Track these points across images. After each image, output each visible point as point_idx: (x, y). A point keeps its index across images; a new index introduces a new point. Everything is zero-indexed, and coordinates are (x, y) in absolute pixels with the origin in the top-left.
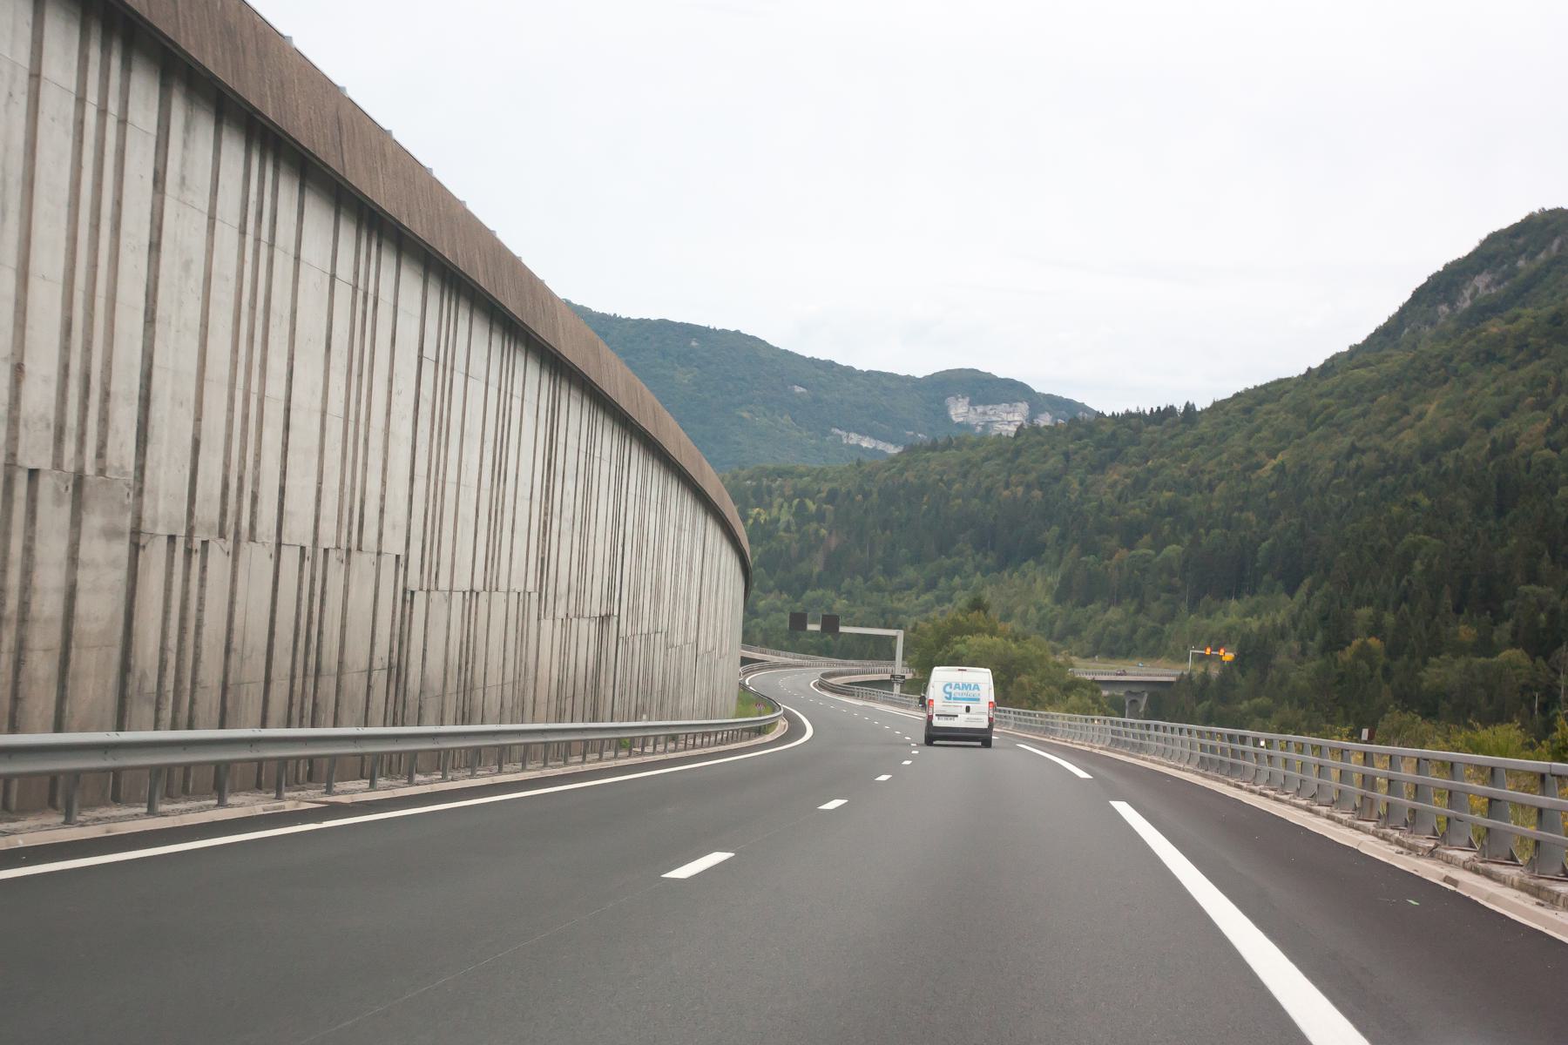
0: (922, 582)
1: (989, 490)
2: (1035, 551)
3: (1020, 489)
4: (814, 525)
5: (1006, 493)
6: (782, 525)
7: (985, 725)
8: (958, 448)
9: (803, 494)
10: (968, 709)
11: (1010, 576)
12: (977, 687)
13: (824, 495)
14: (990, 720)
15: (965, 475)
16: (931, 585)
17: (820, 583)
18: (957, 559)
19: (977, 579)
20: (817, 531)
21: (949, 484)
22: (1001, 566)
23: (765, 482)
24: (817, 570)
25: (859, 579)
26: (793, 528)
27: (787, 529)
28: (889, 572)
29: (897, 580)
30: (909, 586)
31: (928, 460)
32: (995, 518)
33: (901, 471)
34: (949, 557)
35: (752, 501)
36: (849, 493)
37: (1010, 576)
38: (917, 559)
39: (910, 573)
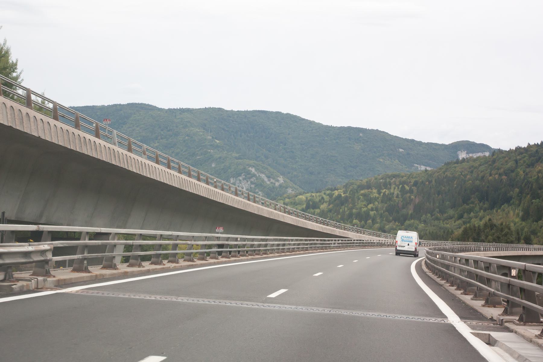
0: (456, 216)
1: (483, 177)
2: (508, 200)
3: (497, 176)
4: (409, 195)
5: (490, 178)
6: (395, 195)
7: (414, 250)
8: (468, 162)
10: (408, 245)
11: (497, 211)
12: (412, 238)
13: (412, 183)
14: (416, 248)
15: (472, 172)
16: (461, 217)
17: (412, 217)
18: (471, 205)
19: (481, 213)
20: (410, 197)
21: (465, 176)
22: (492, 207)
23: (388, 180)
24: (410, 212)
25: (429, 215)
26: (400, 196)
27: (397, 197)
28: (442, 212)
29: (446, 215)
31: (455, 167)
32: (488, 187)
33: (444, 173)
34: (468, 204)
36: (422, 182)
37: (497, 211)
38: (453, 206)
39: (451, 212)
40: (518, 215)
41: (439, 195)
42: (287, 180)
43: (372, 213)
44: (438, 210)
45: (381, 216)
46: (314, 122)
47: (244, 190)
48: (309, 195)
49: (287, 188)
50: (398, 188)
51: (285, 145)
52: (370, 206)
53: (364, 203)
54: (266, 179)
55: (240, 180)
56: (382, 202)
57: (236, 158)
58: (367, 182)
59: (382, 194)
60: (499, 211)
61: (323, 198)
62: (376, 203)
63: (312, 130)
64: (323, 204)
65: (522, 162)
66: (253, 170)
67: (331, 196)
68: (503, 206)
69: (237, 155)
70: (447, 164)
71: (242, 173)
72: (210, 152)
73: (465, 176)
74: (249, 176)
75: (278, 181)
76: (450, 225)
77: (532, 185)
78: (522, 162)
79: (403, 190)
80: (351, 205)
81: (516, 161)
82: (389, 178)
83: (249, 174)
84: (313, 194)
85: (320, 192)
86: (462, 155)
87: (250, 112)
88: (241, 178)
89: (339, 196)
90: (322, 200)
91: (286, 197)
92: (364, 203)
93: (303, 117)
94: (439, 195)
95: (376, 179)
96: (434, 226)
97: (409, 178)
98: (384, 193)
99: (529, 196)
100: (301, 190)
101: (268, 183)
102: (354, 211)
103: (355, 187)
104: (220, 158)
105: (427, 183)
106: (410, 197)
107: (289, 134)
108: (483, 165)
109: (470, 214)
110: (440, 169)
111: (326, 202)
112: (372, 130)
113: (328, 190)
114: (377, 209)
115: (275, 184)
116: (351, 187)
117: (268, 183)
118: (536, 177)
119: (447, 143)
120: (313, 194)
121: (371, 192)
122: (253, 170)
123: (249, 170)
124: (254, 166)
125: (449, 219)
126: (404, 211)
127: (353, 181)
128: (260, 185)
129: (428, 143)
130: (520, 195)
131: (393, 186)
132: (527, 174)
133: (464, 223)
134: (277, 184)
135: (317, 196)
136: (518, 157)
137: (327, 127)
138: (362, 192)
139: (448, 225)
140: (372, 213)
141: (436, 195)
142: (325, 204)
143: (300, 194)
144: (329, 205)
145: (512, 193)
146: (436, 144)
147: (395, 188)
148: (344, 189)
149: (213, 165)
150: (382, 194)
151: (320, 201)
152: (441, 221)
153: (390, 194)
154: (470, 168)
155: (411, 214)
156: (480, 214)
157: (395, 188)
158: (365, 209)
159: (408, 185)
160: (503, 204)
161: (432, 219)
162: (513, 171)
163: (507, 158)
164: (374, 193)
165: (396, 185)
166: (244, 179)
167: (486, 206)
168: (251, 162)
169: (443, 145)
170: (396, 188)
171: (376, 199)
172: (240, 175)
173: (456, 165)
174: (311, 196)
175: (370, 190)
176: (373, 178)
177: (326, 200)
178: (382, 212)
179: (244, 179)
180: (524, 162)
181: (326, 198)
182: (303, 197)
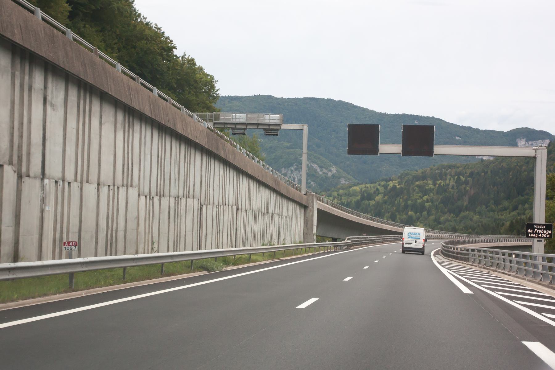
0: (511, 207)
4: (464, 186)
6: (450, 187)
7: (421, 247)
9: (459, 174)
10: (416, 242)
12: (419, 234)
13: (468, 174)
14: (423, 245)
16: (515, 208)
17: (467, 209)
18: (526, 197)
20: (465, 188)
23: (444, 170)
24: (465, 204)
25: (484, 206)
26: (455, 188)
27: (453, 188)
28: (497, 203)
29: (500, 207)
30: (505, 209)
34: (522, 196)
35: (438, 178)
36: (478, 173)
38: (509, 198)
39: (506, 203)
41: (494, 187)
43: (427, 205)
46: (367, 109)
48: (363, 186)
49: (339, 178)
50: (454, 179)
51: (337, 133)
52: (425, 198)
54: (318, 169)
55: (292, 171)
56: (437, 193)
57: (288, 148)
58: (422, 173)
59: (437, 185)
61: (377, 189)
62: (432, 195)
63: (365, 118)
64: (377, 195)
67: (385, 187)
69: (288, 145)
72: (260, 142)
75: (331, 171)
79: (458, 181)
80: (406, 197)
84: (368, 185)
85: (375, 183)
89: (394, 187)
90: (377, 192)
93: (356, 104)
94: (494, 187)
95: (431, 169)
98: (440, 184)
101: (321, 173)
102: (409, 202)
103: (410, 177)
104: (271, 147)
105: (483, 174)
106: (465, 188)
107: (341, 123)
109: (524, 205)
111: (381, 194)
112: (428, 118)
114: (432, 201)
115: (327, 174)
117: (321, 173)
119: (505, 130)
120: (368, 185)
126: (459, 203)
129: (486, 131)
131: (449, 177)
134: (330, 174)
137: (381, 114)
138: (417, 183)
140: (427, 205)
141: (492, 187)
142: (379, 195)
143: (355, 185)
144: (384, 196)
147: (450, 180)
150: (437, 185)
151: (375, 192)
152: (496, 213)
157: (450, 180)
158: (420, 201)
166: (296, 169)
170: (452, 179)
171: (431, 190)
174: (365, 187)
175: (425, 181)
179: (296, 169)
181: (381, 189)
182: (357, 188)
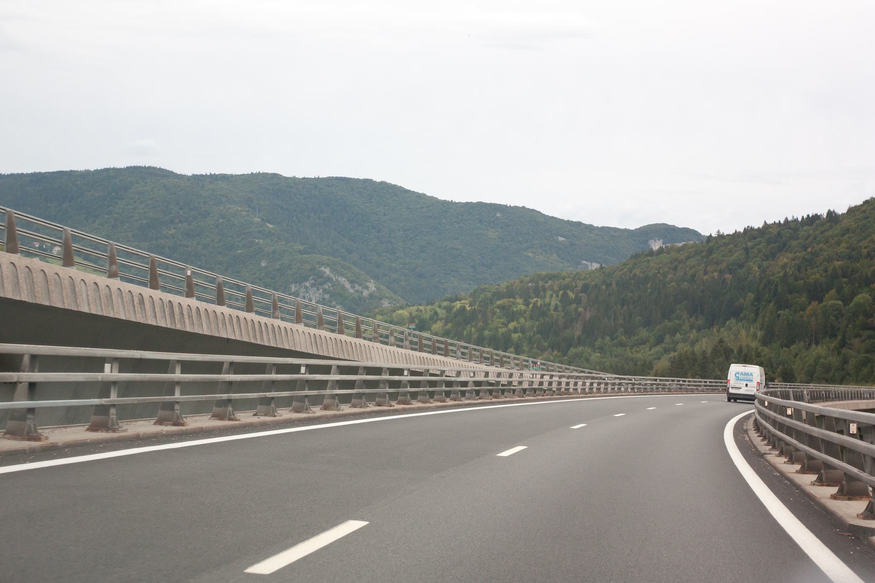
1: (693, 276)
2: (735, 313)
3: (716, 274)
4: (574, 306)
5: (706, 277)
6: (552, 307)
8: (668, 252)
9: (565, 288)
11: (718, 331)
15: (675, 269)
16: (660, 340)
17: (580, 342)
18: (677, 322)
19: (693, 335)
20: (576, 309)
21: (665, 275)
22: (710, 325)
24: (577, 333)
25: (608, 338)
26: (560, 309)
27: (556, 309)
28: (629, 332)
29: (636, 338)
30: (644, 342)
31: (648, 261)
32: (703, 291)
33: (630, 270)
34: (670, 320)
35: (532, 295)
37: (718, 331)
38: (648, 323)
39: (644, 333)
40: (755, 336)
41: (623, 306)
42: (382, 287)
43: (515, 336)
44: (622, 330)
45: (530, 341)
46: (424, 195)
47: (313, 302)
48: (415, 308)
49: (381, 299)
50: (557, 296)
51: (379, 232)
52: (512, 325)
53: (502, 320)
54: (348, 286)
55: (306, 288)
56: (531, 318)
57: (300, 252)
58: (507, 287)
59: (531, 306)
60: (722, 329)
61: (436, 313)
62: (522, 320)
63: (422, 208)
64: (435, 322)
65: (755, 250)
66: (327, 271)
67: (449, 309)
68: (728, 323)
69: (302, 248)
70: (636, 256)
71: (309, 276)
72: (258, 244)
73: (665, 275)
74: (320, 280)
75: (367, 288)
76: (642, 354)
77: (776, 286)
78: (755, 250)
79: (565, 299)
80: (481, 324)
81: (747, 250)
82: (542, 280)
83: (321, 277)
84: (422, 308)
85: (432, 304)
86: (656, 246)
87: (323, 179)
88: (307, 284)
89: (463, 309)
90: (435, 317)
91: (378, 313)
92: (502, 320)
93: (407, 187)
94: (623, 306)
95: (522, 282)
96: (616, 356)
97: (574, 279)
98: (535, 304)
99: (772, 304)
100: (404, 302)
101: (352, 291)
102: (486, 333)
103: (489, 295)
104: (274, 252)
105: (604, 287)
106: (576, 309)
107: (385, 215)
108: (693, 257)
109: (674, 336)
110: (625, 264)
111: (441, 320)
112: (516, 208)
113: (445, 300)
114: (523, 330)
115: (362, 293)
116: (482, 296)
117: (352, 291)
118: (781, 274)
120: (422, 308)
121: (514, 303)
122: (327, 271)
123: (321, 272)
124: (328, 265)
125: (640, 344)
126: (567, 333)
127: (486, 286)
128: (338, 296)
130: (756, 303)
131: (549, 293)
132: (764, 271)
133: (666, 351)
134: (366, 293)
135: (426, 310)
136: (749, 244)
137: (445, 203)
138: (499, 302)
139: (639, 355)
140: (515, 336)
141: (619, 306)
142: (439, 322)
143: (402, 308)
144: (446, 324)
145: (742, 300)
146: (616, 230)
147: (551, 296)
148: (471, 299)
149: (263, 264)
150: (531, 306)
151: (431, 318)
152: (628, 349)
153: (545, 306)
154: (672, 263)
155: (579, 338)
156: (692, 336)
157: (551, 296)
158: (504, 330)
159: (572, 291)
160: (728, 319)
161: (614, 346)
162: (741, 266)
163: (731, 246)
164: (520, 305)
165: (554, 292)
166: (313, 285)
167: (699, 322)
168: (325, 258)
169: (626, 230)
170: (554, 295)
171: (521, 313)
172: (306, 279)
173: (649, 258)
174: (417, 310)
175: (511, 300)
176: (517, 281)
177: (440, 315)
178: (532, 334)
179: (313, 285)
180: (760, 251)
181: (442, 313)
182: (404, 313)
